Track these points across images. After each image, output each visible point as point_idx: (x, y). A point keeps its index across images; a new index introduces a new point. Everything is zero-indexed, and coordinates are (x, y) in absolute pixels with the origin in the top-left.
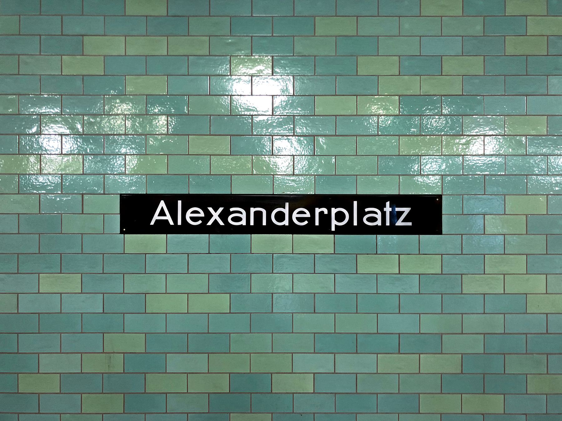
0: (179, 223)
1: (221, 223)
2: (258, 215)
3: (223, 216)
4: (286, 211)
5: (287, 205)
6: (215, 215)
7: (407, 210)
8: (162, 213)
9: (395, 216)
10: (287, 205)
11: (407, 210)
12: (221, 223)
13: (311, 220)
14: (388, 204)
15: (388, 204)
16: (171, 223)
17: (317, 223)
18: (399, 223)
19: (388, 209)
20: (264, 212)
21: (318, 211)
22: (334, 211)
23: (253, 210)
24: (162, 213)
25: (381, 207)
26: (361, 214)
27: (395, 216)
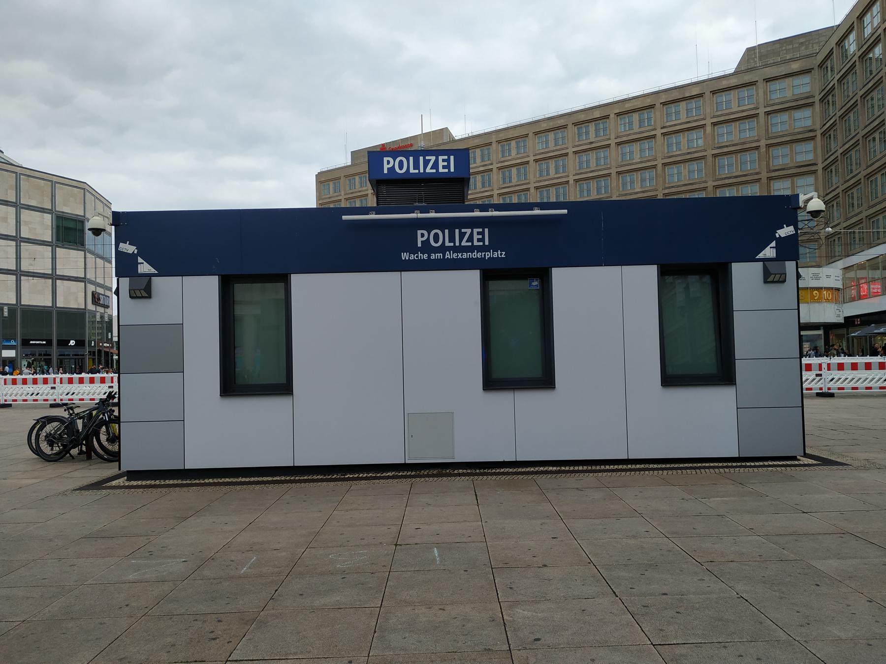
0: (452, 257)
1: (461, 257)
2: (469, 255)
3: (462, 256)
4: (476, 253)
5: (476, 251)
6: (460, 255)
7: (504, 253)
8: (448, 255)
9: (501, 254)
10: (476, 251)
11: (504, 253)
12: (461, 257)
13: (482, 255)
14: (499, 251)
15: (499, 251)
16: (449, 258)
17: (483, 257)
18: (503, 256)
19: (499, 252)
20: (470, 254)
21: (483, 253)
22: (487, 253)
23: (468, 254)
24: (448, 255)
25: (497, 252)
26: (493, 254)
27: (501, 254)
